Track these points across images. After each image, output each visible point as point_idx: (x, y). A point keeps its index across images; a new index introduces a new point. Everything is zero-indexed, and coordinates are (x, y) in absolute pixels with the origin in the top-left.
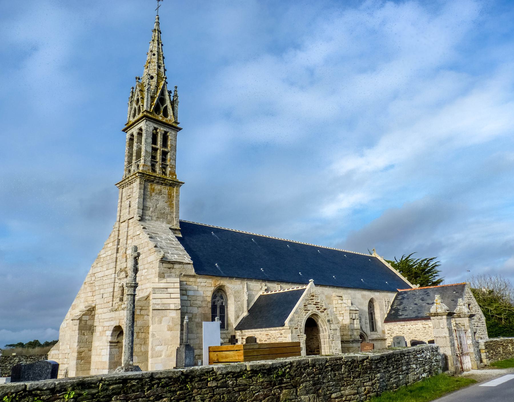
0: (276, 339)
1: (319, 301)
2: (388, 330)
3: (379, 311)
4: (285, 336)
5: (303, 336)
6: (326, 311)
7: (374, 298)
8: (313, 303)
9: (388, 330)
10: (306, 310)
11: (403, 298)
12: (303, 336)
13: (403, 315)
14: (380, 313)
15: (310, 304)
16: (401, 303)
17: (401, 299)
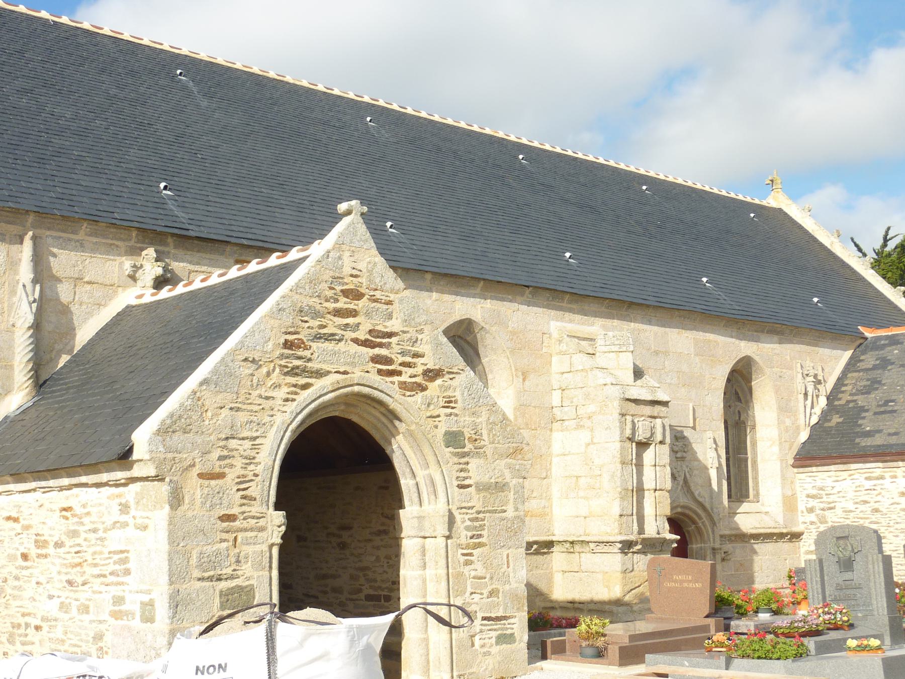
0: (100, 534)
1: (394, 325)
2: (808, 496)
3: (775, 415)
4: (139, 521)
5: (262, 522)
6: (439, 382)
7: (756, 358)
8: (349, 335)
9: (808, 496)
10: (293, 372)
11: (885, 363)
12: (262, 522)
13: (880, 431)
14: (780, 422)
15: (329, 338)
16: (874, 384)
17: (875, 368)
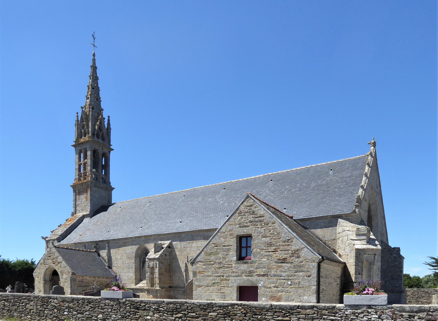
15: (48, 260)
